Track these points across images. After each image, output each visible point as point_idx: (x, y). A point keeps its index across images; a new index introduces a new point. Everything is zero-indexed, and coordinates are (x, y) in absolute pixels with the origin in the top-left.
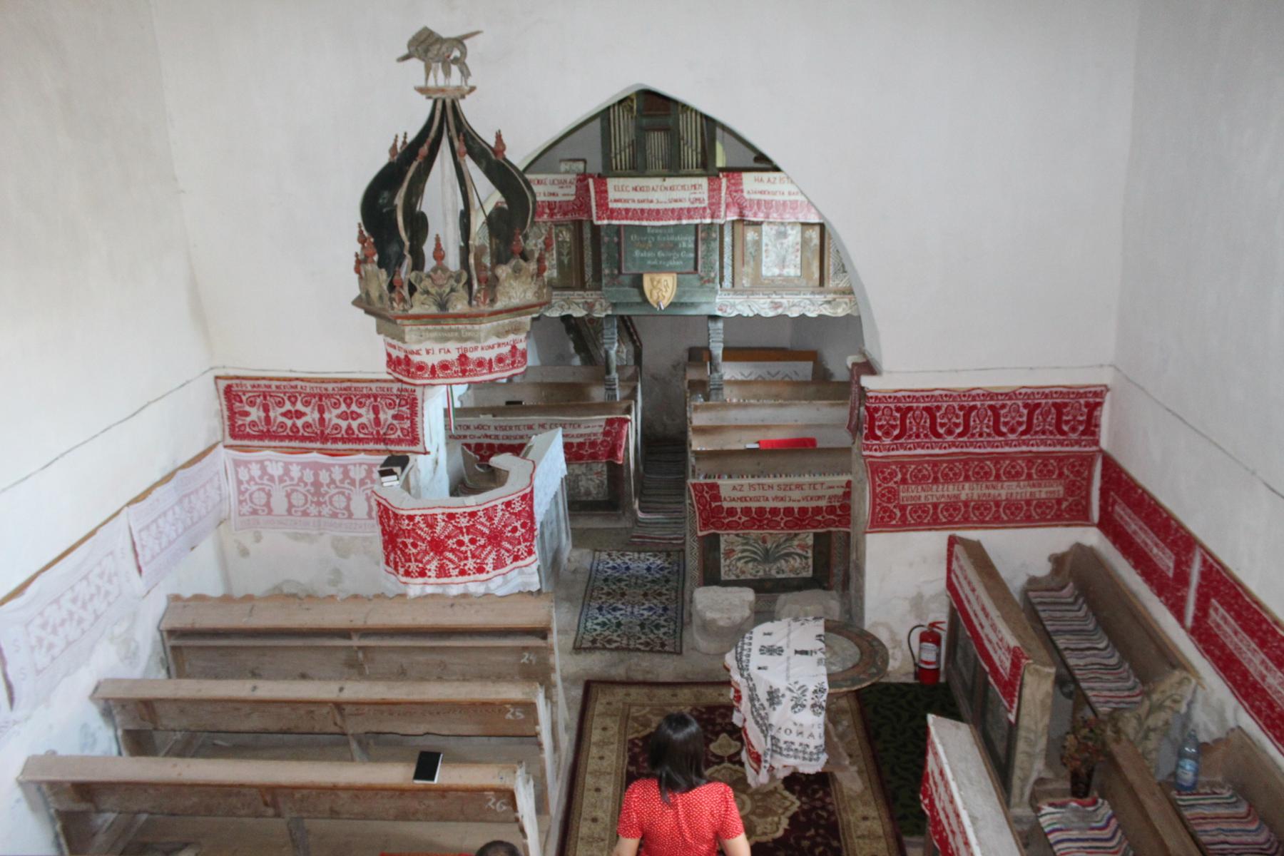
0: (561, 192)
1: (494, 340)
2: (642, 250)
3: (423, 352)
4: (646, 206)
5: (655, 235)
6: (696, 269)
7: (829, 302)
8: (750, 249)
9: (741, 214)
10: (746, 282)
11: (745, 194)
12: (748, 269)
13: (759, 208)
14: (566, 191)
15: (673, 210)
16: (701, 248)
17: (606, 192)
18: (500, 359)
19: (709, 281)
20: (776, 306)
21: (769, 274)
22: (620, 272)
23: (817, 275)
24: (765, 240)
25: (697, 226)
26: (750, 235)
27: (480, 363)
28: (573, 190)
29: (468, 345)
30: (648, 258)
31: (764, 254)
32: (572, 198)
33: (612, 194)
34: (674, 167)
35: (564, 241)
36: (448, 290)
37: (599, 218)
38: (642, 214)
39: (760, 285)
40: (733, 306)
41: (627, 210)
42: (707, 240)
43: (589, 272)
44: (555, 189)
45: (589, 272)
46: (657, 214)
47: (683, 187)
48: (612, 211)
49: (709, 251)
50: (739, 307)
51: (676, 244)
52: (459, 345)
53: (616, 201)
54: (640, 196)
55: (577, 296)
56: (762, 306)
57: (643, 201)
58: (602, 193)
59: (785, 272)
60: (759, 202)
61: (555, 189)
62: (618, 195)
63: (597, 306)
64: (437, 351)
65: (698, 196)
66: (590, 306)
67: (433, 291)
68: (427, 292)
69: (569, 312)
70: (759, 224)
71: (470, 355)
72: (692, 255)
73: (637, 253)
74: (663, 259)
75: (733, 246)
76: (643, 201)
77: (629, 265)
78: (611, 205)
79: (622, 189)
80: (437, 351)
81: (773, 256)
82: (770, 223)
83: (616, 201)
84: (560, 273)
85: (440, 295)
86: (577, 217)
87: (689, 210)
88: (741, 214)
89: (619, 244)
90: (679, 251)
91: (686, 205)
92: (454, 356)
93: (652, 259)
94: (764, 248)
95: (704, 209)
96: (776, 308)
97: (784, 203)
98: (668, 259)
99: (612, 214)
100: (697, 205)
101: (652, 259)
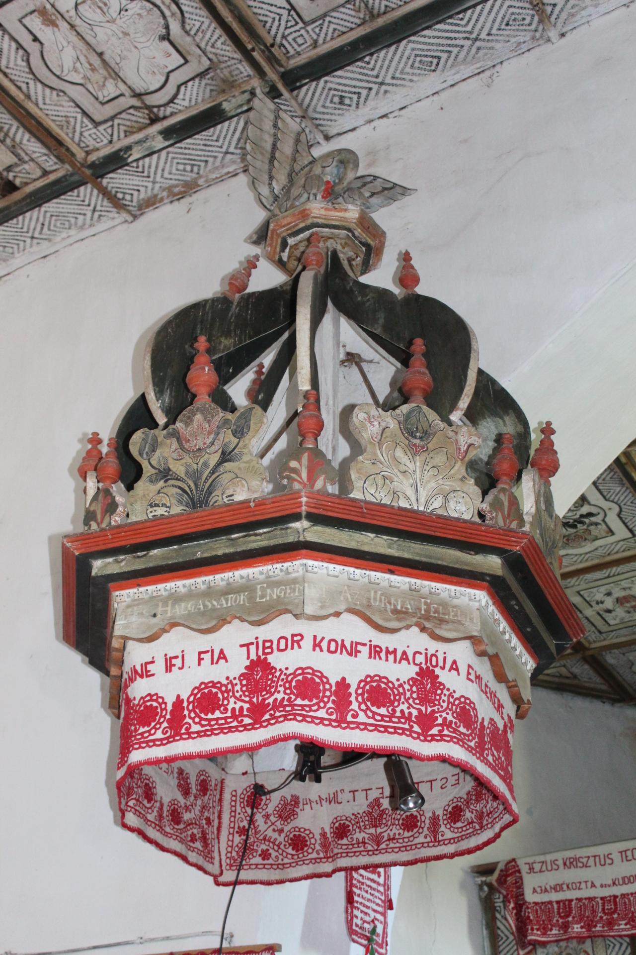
1: (353, 629)
3: (158, 668)
18: (378, 692)
27: (308, 685)
29: (274, 630)
36: (214, 459)
52: (249, 633)
64: (191, 659)
67: (179, 468)
68: (165, 474)
71: (277, 660)
80: (191, 659)
85: (195, 476)
92: (236, 665)
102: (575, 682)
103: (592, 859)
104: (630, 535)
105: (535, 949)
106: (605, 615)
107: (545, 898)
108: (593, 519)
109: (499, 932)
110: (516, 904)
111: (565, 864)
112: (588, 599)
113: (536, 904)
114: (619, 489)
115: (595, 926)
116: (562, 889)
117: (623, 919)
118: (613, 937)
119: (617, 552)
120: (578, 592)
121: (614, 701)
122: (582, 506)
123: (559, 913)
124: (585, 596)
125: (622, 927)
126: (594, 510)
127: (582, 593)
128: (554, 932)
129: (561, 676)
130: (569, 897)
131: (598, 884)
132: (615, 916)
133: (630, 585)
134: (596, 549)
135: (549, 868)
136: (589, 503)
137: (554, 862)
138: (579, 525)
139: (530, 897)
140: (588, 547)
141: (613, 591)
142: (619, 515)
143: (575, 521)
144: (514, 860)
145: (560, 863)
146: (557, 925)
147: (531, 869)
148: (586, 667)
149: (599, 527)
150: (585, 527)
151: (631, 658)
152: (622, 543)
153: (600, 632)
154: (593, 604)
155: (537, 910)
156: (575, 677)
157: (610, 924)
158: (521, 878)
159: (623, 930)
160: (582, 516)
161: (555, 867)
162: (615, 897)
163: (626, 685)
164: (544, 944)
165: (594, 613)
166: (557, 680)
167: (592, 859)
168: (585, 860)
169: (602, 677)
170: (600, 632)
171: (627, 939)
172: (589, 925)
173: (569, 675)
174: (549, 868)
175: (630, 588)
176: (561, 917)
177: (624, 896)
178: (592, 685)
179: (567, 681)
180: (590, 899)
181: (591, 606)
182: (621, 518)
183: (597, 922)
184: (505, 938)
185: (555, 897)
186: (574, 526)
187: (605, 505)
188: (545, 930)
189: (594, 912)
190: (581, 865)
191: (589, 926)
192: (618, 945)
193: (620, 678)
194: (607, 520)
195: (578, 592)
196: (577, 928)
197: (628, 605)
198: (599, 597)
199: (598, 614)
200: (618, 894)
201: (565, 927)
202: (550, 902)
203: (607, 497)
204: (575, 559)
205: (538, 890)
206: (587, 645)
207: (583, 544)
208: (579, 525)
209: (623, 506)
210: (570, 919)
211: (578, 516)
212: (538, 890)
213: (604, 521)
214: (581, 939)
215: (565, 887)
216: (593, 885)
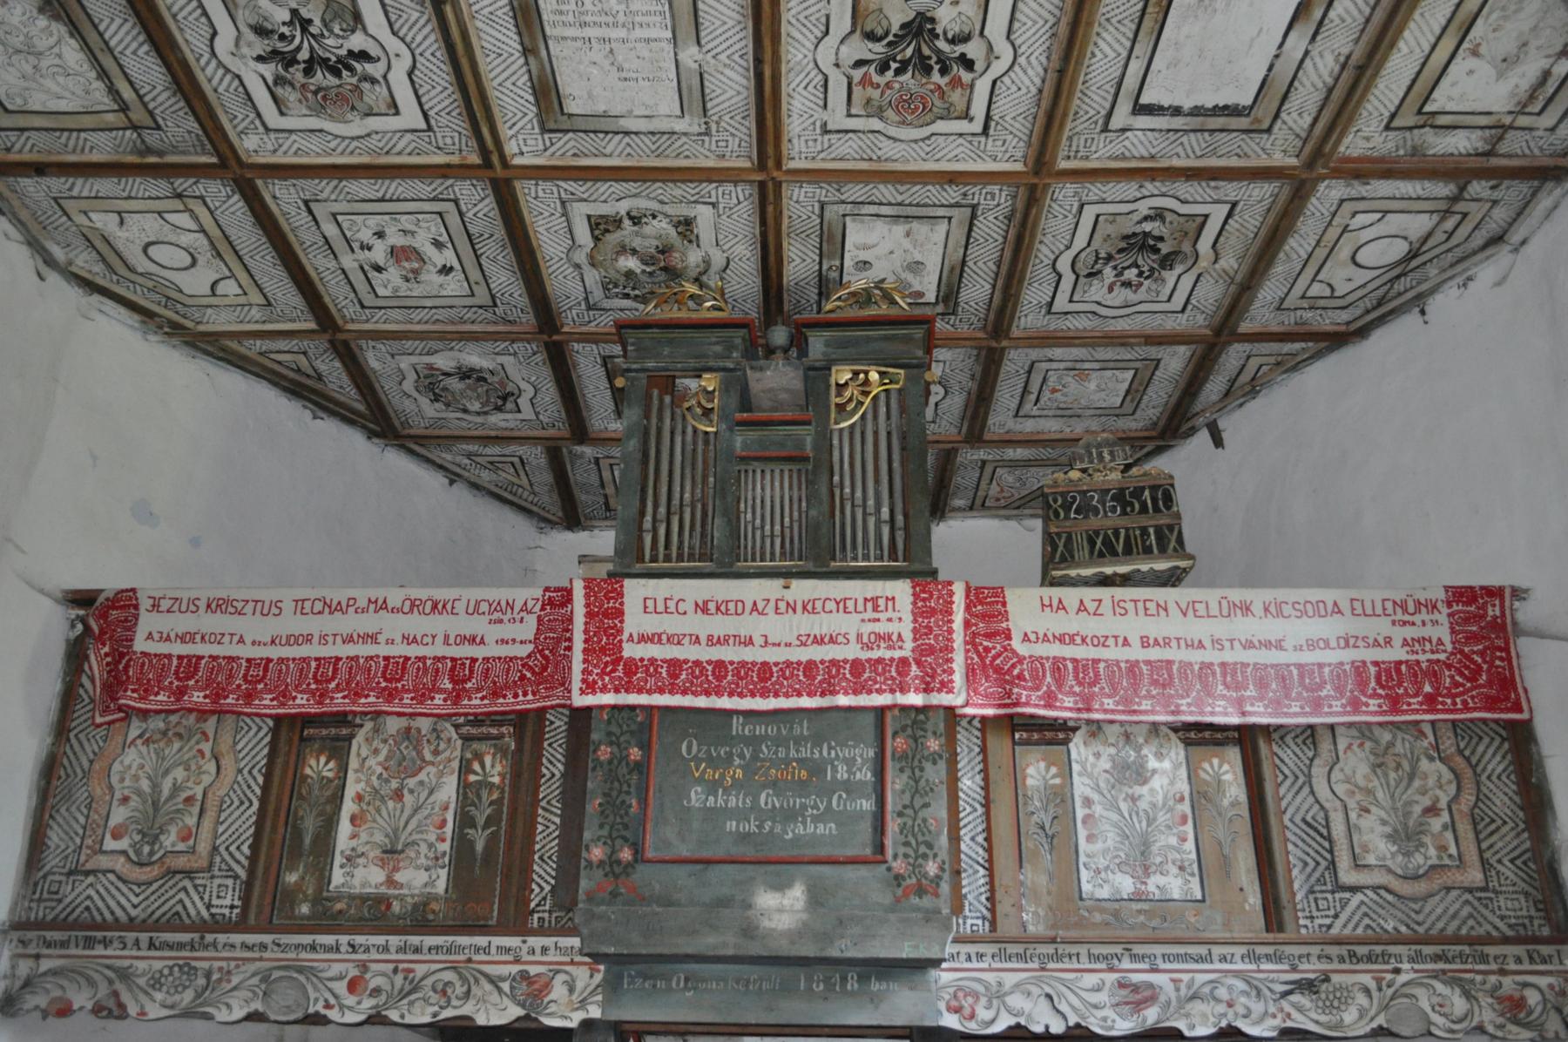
0: (493, 633)
2: (712, 787)
4: (729, 654)
5: (754, 741)
6: (880, 848)
7: (1308, 987)
8: (1038, 813)
9: (1007, 699)
10: (1033, 920)
11: (1016, 644)
12: (1035, 877)
13: (1060, 681)
14: (507, 630)
15: (810, 667)
16: (896, 783)
17: (619, 613)
19: (920, 891)
20: (1139, 997)
21: (1104, 893)
22: (638, 850)
23: (1254, 899)
24: (1081, 787)
25: (881, 711)
26: (1037, 771)
28: (528, 628)
30: (726, 813)
31: (1082, 833)
32: (523, 651)
33: (635, 621)
34: (819, 553)
35: (485, 784)
37: (589, 687)
38: (718, 676)
39: (1076, 931)
40: (997, 996)
41: (675, 665)
42: (912, 761)
43: (543, 875)
44: (478, 625)
45: (543, 875)
46: (763, 677)
47: (841, 605)
48: (631, 666)
49: (917, 788)
50: (1016, 1001)
51: (816, 769)
53: (643, 639)
54: (718, 625)
55: (498, 951)
56: (1091, 995)
57: (722, 641)
58: (606, 614)
59: (1153, 884)
60: (1058, 665)
61: (478, 625)
62: (651, 624)
63: (558, 991)
65: (881, 628)
66: (533, 989)
69: (467, 1009)
70: (1053, 733)
72: (867, 805)
73: (696, 796)
74: (773, 814)
75: (987, 805)
76: (722, 641)
77: (670, 833)
78: (630, 651)
79: (668, 607)
81: (1112, 838)
82: (1096, 729)
83: (643, 639)
84: (456, 880)
86: (527, 702)
87: (857, 666)
88: (1007, 699)
89: (641, 768)
90: (827, 791)
91: (852, 652)
93: (740, 815)
94: (1080, 813)
95: (904, 661)
96: (1138, 1006)
97: (1133, 666)
98: (790, 816)
99: (632, 674)
100: (882, 653)
101: (740, 815)
102: (319, 386)
103: (251, 604)
104: (423, 126)
105: (127, 718)
106: (372, 274)
107: (163, 648)
108: (370, 68)
109: (81, 691)
110: (113, 649)
111: (209, 606)
112: (349, 234)
113: (144, 654)
114: (416, 15)
115: (226, 697)
116: (193, 640)
117: (270, 692)
118: (248, 715)
119: (399, 153)
120: (334, 215)
121: (371, 434)
122: (353, 31)
123: (176, 673)
124: (345, 225)
125: (267, 702)
126: (374, 51)
127: (340, 218)
128: (160, 698)
129: (299, 370)
130: (200, 653)
131: (248, 640)
132: (260, 686)
133: (413, 228)
134: (368, 135)
135: (184, 608)
136: (364, 29)
137: (193, 601)
138: (345, 73)
139: (140, 645)
140: (357, 126)
141: (387, 230)
142: (410, 74)
143: (339, 61)
144: (133, 590)
145: (202, 604)
146: (169, 688)
147: (155, 606)
148: (337, 364)
149: (377, 88)
150: (354, 80)
151: (402, 366)
152: (409, 136)
153: (363, 307)
154: (356, 246)
155: (143, 664)
156: (320, 378)
157: (249, 697)
158: (136, 617)
159: (266, 707)
160: (350, 52)
161: (192, 608)
162: (269, 660)
163: (392, 415)
164: (144, 714)
165: (356, 265)
166: (291, 375)
167: (251, 604)
168: (239, 605)
169: (358, 387)
170: (363, 307)
171: (271, 723)
172: (217, 695)
173: (312, 373)
174: (184, 608)
175: (413, 233)
176: (178, 679)
177: (281, 660)
178: (342, 399)
179: (309, 382)
180: (231, 659)
181: (353, 251)
182: (412, 82)
183: (232, 692)
184: (87, 701)
185: (178, 649)
186: (337, 73)
187: (393, 44)
188: (146, 692)
189: (231, 676)
190: (231, 609)
191: (217, 696)
192: (255, 729)
193: (383, 397)
194: (390, 76)
195: (334, 215)
196: (198, 697)
197: (406, 264)
198: (366, 235)
199: (362, 268)
200: (275, 657)
201: (181, 692)
202: (169, 657)
203: (396, 27)
204: (332, 145)
205: (156, 636)
206: (340, 322)
207: (349, 116)
208: (345, 73)
209: (418, 58)
210: (192, 683)
211: (343, 52)
212: (156, 636)
213: (385, 77)
214: (203, 714)
215: (198, 638)
216: (241, 641)
